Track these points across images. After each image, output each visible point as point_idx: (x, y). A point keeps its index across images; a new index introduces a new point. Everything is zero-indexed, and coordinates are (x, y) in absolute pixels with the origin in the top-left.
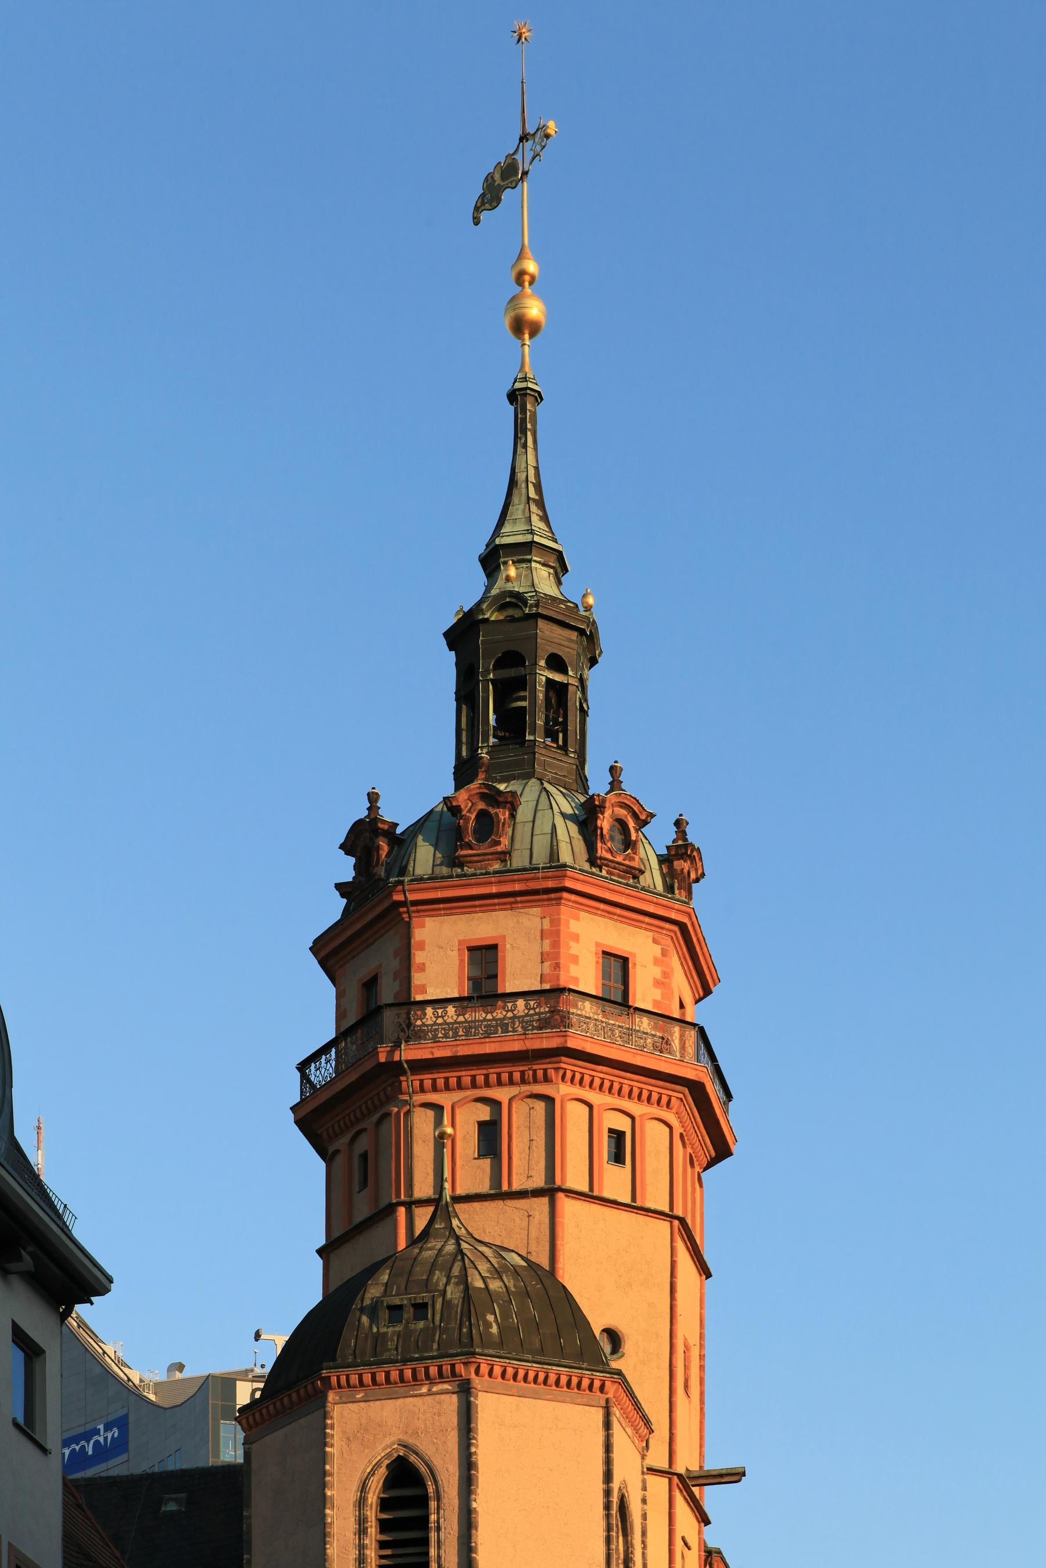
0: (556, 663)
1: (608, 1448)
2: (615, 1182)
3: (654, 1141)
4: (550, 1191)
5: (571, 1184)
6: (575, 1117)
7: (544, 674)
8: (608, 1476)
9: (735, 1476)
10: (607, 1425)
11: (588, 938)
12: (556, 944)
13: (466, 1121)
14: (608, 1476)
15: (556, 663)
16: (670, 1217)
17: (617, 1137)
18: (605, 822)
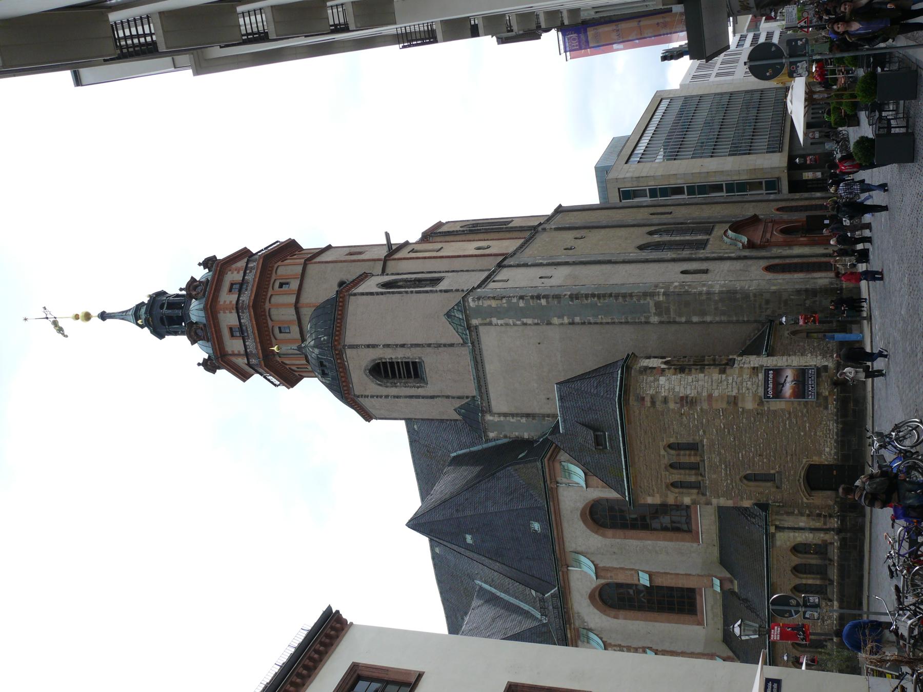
1: (362, 294)
10: (355, 295)
14: (372, 294)
15: (162, 307)
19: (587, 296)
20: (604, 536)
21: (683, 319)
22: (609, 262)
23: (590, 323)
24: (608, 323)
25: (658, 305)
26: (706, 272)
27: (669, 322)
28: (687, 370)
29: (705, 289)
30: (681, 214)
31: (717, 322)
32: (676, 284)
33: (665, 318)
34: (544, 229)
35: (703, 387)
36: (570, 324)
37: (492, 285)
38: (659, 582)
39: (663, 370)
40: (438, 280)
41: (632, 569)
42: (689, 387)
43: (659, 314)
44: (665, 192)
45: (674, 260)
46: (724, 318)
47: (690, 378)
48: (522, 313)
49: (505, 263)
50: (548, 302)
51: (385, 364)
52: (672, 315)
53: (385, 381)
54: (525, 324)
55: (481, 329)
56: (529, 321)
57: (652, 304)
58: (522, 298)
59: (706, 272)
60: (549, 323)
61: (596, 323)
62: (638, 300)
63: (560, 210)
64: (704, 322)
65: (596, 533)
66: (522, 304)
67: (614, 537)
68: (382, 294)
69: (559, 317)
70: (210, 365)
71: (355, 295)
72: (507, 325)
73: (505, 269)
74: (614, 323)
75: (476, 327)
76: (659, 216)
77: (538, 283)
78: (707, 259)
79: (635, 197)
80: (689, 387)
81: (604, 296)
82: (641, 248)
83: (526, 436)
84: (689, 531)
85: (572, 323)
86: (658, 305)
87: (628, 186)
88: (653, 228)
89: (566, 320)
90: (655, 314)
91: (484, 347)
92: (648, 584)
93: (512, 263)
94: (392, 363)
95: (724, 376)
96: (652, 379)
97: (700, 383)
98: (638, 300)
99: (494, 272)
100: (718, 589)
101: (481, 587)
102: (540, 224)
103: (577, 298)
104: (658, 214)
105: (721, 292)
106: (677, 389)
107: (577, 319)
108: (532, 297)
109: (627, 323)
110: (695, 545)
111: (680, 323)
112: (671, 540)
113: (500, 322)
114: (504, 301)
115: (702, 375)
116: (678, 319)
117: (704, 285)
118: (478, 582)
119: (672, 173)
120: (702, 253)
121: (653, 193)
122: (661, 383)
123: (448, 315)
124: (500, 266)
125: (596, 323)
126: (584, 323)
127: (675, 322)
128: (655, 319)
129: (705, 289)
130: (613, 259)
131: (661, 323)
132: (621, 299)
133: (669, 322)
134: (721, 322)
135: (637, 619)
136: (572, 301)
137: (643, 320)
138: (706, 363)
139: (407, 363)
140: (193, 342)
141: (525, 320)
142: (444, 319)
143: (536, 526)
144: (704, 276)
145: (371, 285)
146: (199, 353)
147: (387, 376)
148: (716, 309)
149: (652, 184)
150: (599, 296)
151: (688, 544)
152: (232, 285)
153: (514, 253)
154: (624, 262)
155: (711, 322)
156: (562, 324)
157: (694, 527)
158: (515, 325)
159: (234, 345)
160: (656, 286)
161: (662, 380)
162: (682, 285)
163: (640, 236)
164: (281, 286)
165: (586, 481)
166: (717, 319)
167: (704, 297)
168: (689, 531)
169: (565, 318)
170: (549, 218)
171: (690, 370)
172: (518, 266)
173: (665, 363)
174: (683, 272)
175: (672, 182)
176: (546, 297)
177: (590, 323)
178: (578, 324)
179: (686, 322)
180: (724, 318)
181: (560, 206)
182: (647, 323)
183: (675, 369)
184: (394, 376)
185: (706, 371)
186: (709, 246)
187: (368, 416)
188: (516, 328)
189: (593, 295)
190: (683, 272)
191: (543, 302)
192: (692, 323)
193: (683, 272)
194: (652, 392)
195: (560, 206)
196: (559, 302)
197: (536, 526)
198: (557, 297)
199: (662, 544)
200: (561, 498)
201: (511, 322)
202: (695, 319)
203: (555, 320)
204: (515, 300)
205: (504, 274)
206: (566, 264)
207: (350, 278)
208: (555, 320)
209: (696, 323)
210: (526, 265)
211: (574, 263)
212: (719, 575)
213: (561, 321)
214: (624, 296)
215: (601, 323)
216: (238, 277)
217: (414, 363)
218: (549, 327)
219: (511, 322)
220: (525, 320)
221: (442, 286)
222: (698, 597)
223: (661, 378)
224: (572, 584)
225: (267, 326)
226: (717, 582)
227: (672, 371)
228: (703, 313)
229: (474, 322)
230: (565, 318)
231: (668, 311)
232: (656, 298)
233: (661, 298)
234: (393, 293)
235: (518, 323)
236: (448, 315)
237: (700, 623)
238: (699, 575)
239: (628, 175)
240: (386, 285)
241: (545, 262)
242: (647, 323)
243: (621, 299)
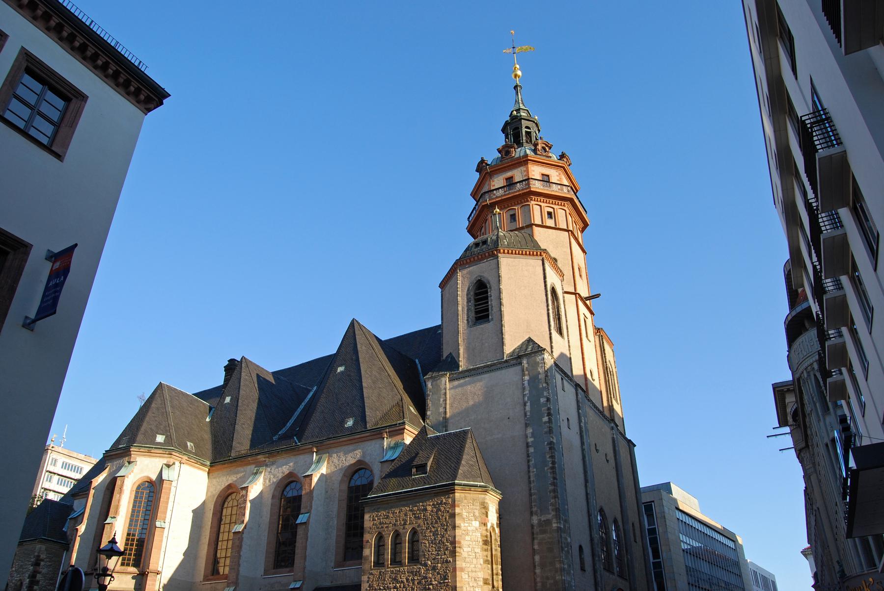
0: (527, 127)
2: (550, 223)
3: (561, 214)
4: (530, 226)
5: (536, 222)
6: (536, 209)
7: (524, 130)
8: (545, 278)
9: (597, 296)
11: (536, 171)
12: (528, 172)
13: (506, 216)
15: (527, 127)
16: (568, 231)
17: (549, 214)
18: (539, 147)
19: (552, 457)
20: (341, 482)
21: (536, 547)
22: (586, 481)
23: (529, 461)
24: (529, 477)
25: (548, 522)
26: (583, 569)
27: (533, 533)
28: (486, 547)
29: (566, 566)
30: (637, 550)
31: (535, 579)
32: (569, 540)
33: (536, 530)
34: (612, 428)
35: (471, 563)
36: (527, 444)
37: (558, 377)
38: (300, 531)
39: (485, 524)
40: (560, 332)
41: (311, 507)
42: (470, 549)
43: (540, 524)
44: (654, 542)
45: (592, 540)
46: (539, 585)
47: (478, 550)
48: (535, 402)
49: (580, 391)
50: (545, 423)
51: (487, 292)
52: (540, 536)
53: (472, 293)
54: (525, 405)
55: (518, 368)
56: (528, 408)
57: (549, 517)
58: (548, 400)
59: (583, 569)
60: (527, 425)
61: (529, 467)
62: (552, 504)
63: (631, 445)
64: (535, 567)
65: (344, 475)
66: (543, 400)
67: (340, 491)
68: (546, 286)
69: (532, 433)
70: (481, 167)
71: (543, 264)
72: (524, 389)
73: (574, 390)
74: (530, 482)
75: (520, 363)
76: (631, 530)
77: (563, 416)
78: (595, 571)
79: (648, 516)
80: (470, 549)
81: (554, 473)
82: (601, 511)
83: (429, 413)
84: (345, 560)
85: (528, 446)
86: (548, 522)
87: (656, 509)
88: (620, 523)
89: (530, 440)
90: (540, 520)
91: (503, 371)
92: (298, 521)
93: (580, 396)
94: (487, 298)
95: (481, 583)
96: (477, 514)
97: (475, 561)
98: (552, 504)
99: (571, 380)
100: (292, 586)
101: (309, 391)
102: (617, 426)
103: (550, 448)
104: (634, 530)
105: (563, 582)
106: (468, 538)
107: (531, 450)
108: (549, 409)
109: (531, 495)
110: (333, 564)
111: (533, 545)
112: (337, 542)
113: (526, 383)
114: (544, 385)
115: (482, 561)
116: (536, 541)
117: (569, 566)
118: (315, 388)
119: (672, 547)
120: (600, 567)
121: (652, 532)
122: (474, 522)
123: (530, 340)
124: (577, 386)
125: (529, 467)
126: (528, 456)
127: (533, 539)
128: (535, 520)
129: (566, 566)
130: (589, 485)
131: (532, 526)
132: (551, 488)
133: (533, 533)
134: (536, 583)
135: (271, 516)
136: (548, 444)
137: (534, 509)
138: (494, 566)
139: (487, 310)
140: (499, 151)
141: (528, 404)
142: (526, 338)
143: (350, 423)
144: (578, 567)
145: (553, 278)
146: (492, 157)
147: (476, 294)
148: (548, 578)
149: (660, 530)
150: (553, 468)
151: (333, 558)
152: (548, 176)
153: (589, 400)
154: (587, 494)
155: (535, 573)
156: (527, 437)
157: (348, 563)
158: (524, 396)
159: (498, 181)
160: (566, 521)
161: (476, 524)
162: (569, 545)
163: (613, 510)
164: (549, 214)
165: (387, 461)
166: (538, 580)
167: (558, 566)
168: (345, 560)
169: (532, 439)
170: (623, 435)
171: (486, 550)
172: (578, 401)
173: (492, 527)
174: (580, 547)
175: (663, 548)
176: (550, 421)
177: (529, 461)
178: (528, 451)
179: (534, 549)
180: (539, 585)
181: (635, 446)
182: (532, 513)
183: (486, 536)
184: (476, 300)
185: (485, 565)
186: (608, 574)
187: (442, 285)
188: (521, 397)
189: (553, 463)
190: (580, 547)
191: (546, 419)
192: (534, 555)
193: (581, 547)
194: (465, 514)
195: (635, 446)
196: (546, 433)
197: (350, 423)
198: (550, 431)
199: (334, 533)
200: (374, 442)
201: (527, 392)
202: (537, 558)
203: (530, 431)
204: (545, 394)
205: (570, 389)
206: (582, 443)
207: (560, 264)
208: (530, 431)
209: (534, 559)
210: (579, 408)
211: (583, 450)
212: (304, 587)
213: (530, 435)
214: (554, 491)
215: (529, 472)
216: (553, 180)
217: (487, 316)
218: (524, 425)
219: (527, 392)
220: (528, 404)
221: (555, 335)
222: (288, 569)
223: (478, 523)
224: (302, 457)
225: (515, 205)
226: (298, 585)
227: (484, 533)
228: (543, 565)
229: (525, 362)
230: (532, 439)
231: (543, 532)
232: (554, 521)
233: (554, 525)
234: (546, 295)
235: (526, 399)
236: (530, 340)
237: (266, 572)
238: (304, 568)
239: (666, 509)
240: (553, 290)
241: (582, 424)
242: (532, 513)
243: (551, 488)
